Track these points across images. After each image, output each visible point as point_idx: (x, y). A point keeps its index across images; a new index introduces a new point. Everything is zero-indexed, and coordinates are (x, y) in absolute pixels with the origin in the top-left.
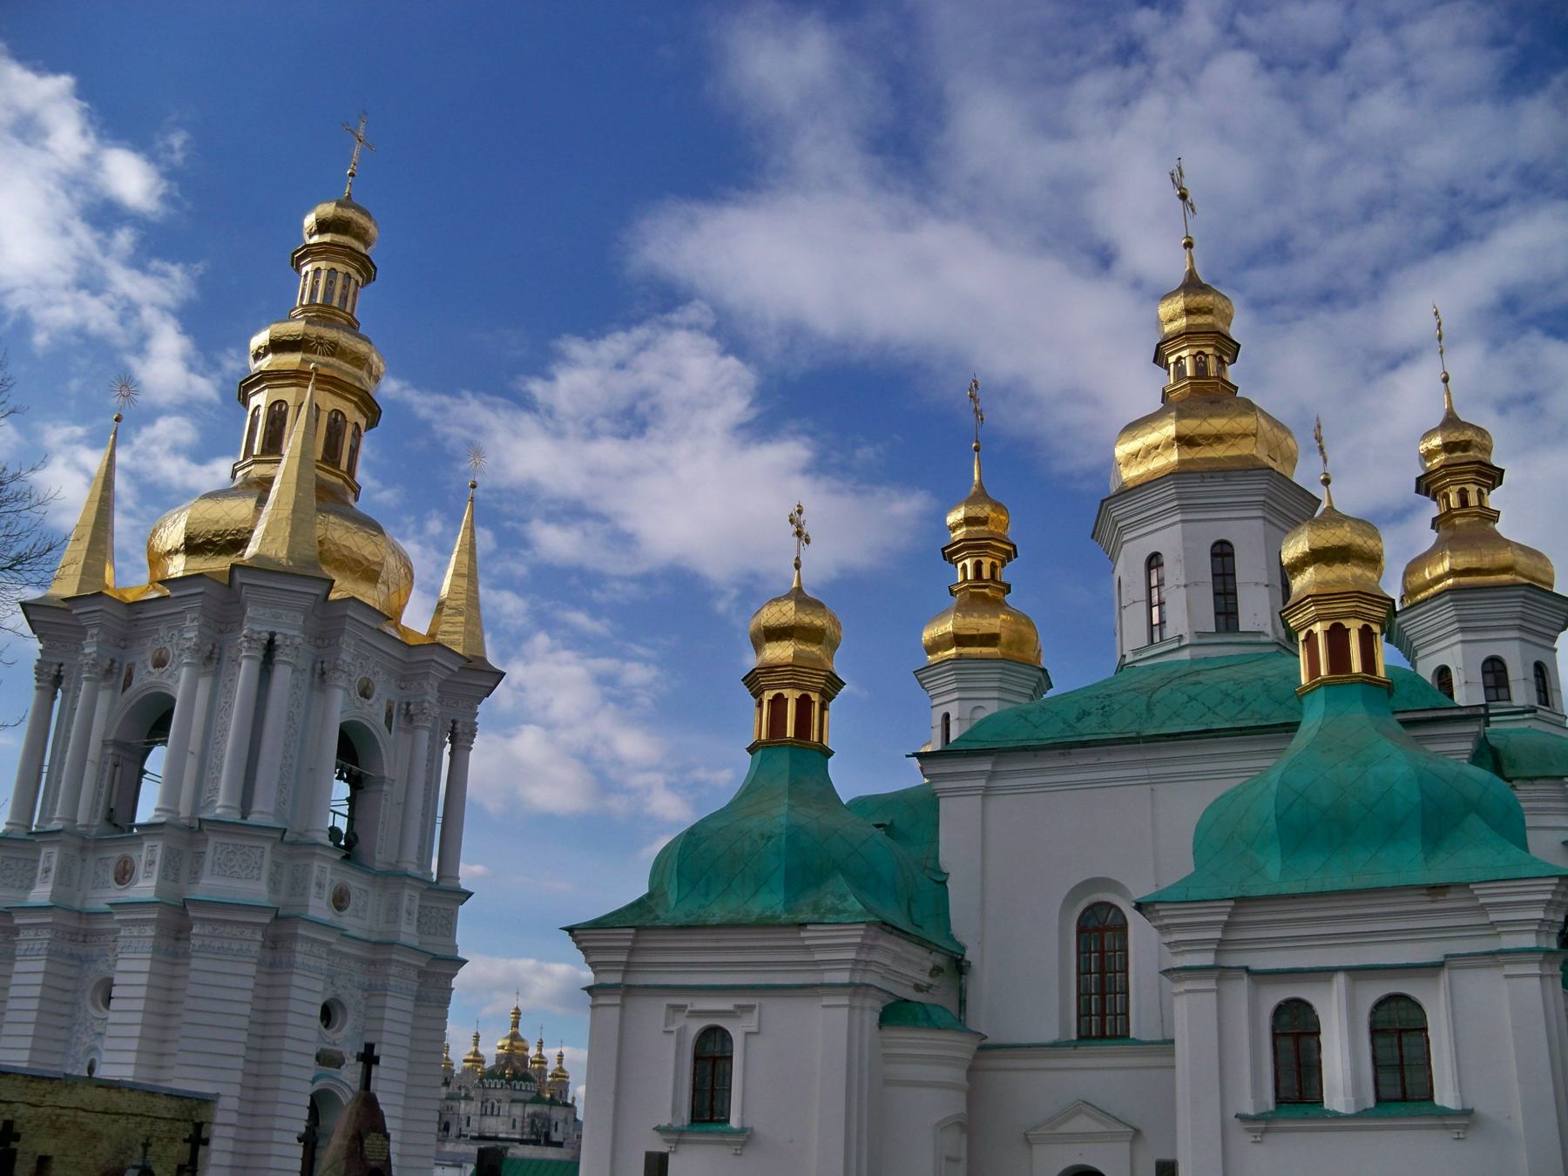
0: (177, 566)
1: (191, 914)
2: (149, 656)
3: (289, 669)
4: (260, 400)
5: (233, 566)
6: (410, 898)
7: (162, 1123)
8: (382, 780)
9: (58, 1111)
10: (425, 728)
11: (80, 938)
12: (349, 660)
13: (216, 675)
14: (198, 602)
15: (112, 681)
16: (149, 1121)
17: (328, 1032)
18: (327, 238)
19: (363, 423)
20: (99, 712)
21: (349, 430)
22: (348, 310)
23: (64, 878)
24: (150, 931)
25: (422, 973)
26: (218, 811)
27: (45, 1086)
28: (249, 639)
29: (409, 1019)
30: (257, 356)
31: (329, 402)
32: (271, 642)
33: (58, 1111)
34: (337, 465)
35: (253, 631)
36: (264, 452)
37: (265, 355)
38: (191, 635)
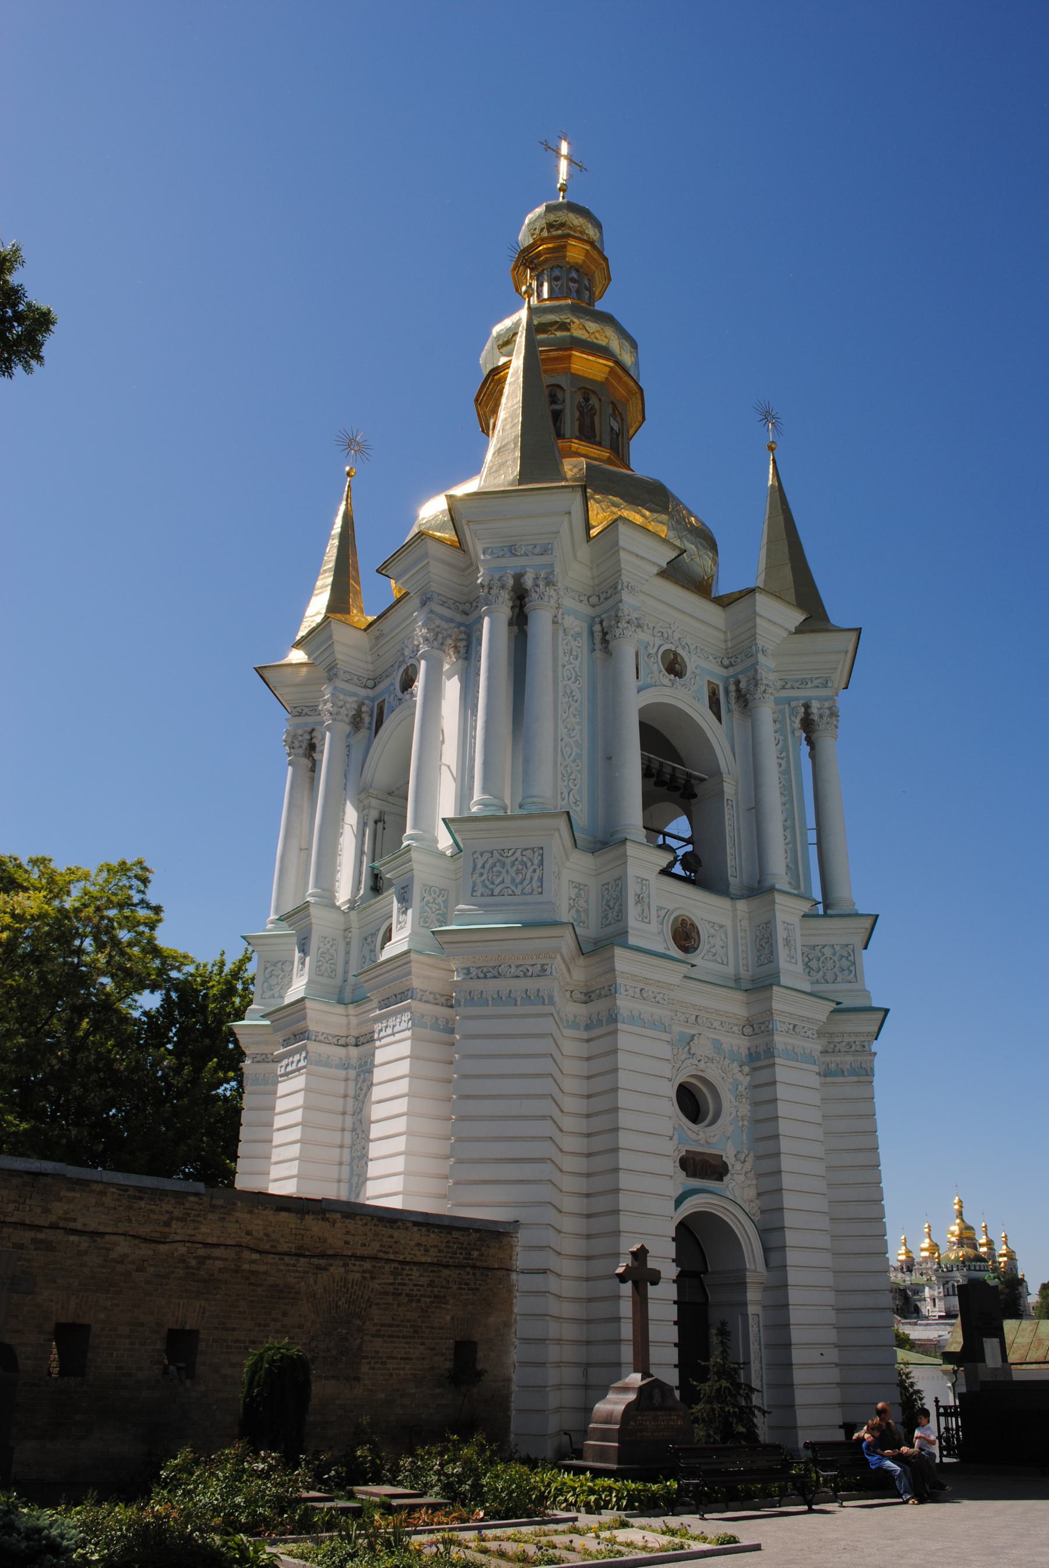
7: (415, 1273)
9: (202, 1252)
16: (388, 1268)
26: (474, 809)
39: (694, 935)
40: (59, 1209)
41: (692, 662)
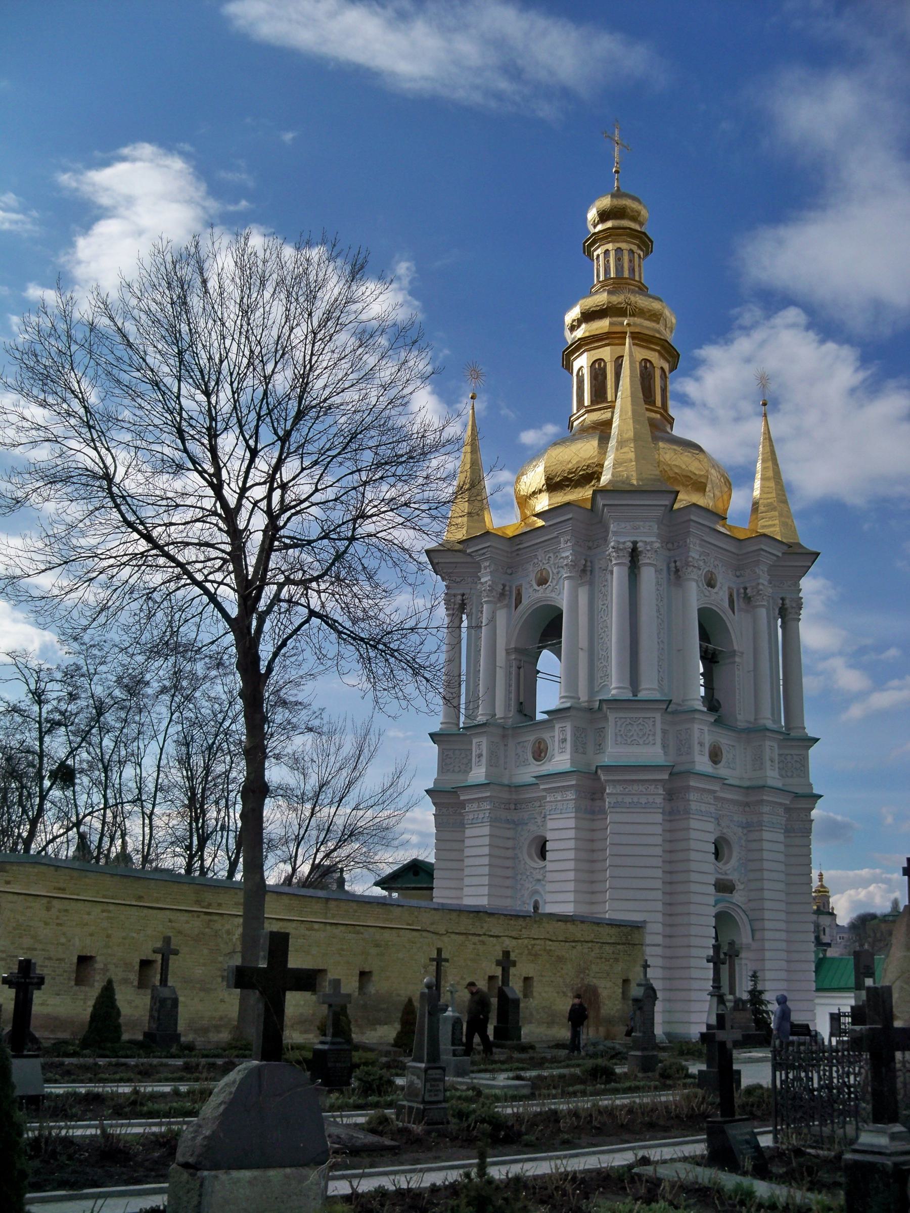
0: (543, 503)
1: (603, 778)
2: (532, 578)
3: (652, 569)
4: (582, 362)
5: (595, 492)
6: (771, 748)
7: (607, 947)
8: (733, 653)
9: (533, 942)
10: (763, 606)
11: (512, 806)
12: (697, 557)
13: (591, 584)
14: (568, 527)
15: (506, 602)
17: (720, 865)
18: (609, 224)
19: (666, 366)
20: (501, 627)
21: (658, 373)
22: (637, 278)
23: (493, 761)
24: (571, 795)
25: (788, 810)
26: (614, 692)
27: (521, 922)
28: (616, 549)
29: (781, 848)
30: (573, 328)
33: (533, 942)
34: (653, 403)
35: (618, 542)
36: (593, 402)
37: (579, 326)
38: (568, 554)
39: (719, 753)
40: (485, 926)
41: (720, 579)
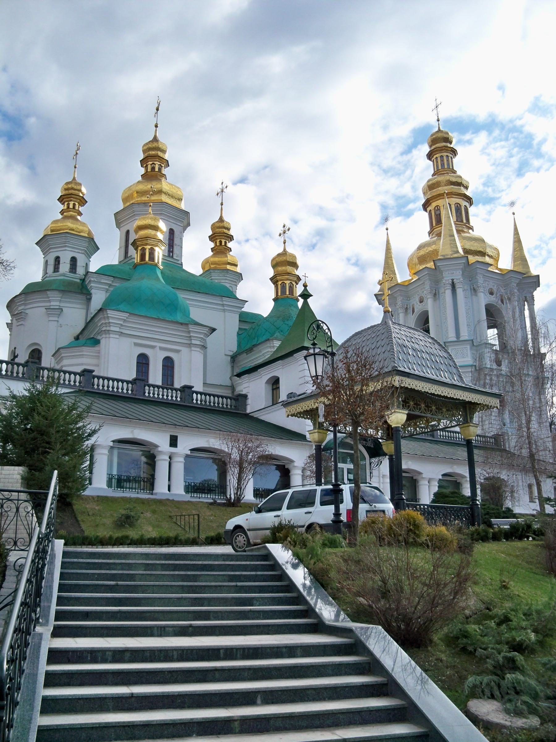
22: (451, 168)
31: (454, 200)
32: (453, 283)
34: (462, 221)
